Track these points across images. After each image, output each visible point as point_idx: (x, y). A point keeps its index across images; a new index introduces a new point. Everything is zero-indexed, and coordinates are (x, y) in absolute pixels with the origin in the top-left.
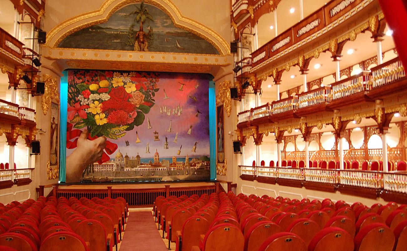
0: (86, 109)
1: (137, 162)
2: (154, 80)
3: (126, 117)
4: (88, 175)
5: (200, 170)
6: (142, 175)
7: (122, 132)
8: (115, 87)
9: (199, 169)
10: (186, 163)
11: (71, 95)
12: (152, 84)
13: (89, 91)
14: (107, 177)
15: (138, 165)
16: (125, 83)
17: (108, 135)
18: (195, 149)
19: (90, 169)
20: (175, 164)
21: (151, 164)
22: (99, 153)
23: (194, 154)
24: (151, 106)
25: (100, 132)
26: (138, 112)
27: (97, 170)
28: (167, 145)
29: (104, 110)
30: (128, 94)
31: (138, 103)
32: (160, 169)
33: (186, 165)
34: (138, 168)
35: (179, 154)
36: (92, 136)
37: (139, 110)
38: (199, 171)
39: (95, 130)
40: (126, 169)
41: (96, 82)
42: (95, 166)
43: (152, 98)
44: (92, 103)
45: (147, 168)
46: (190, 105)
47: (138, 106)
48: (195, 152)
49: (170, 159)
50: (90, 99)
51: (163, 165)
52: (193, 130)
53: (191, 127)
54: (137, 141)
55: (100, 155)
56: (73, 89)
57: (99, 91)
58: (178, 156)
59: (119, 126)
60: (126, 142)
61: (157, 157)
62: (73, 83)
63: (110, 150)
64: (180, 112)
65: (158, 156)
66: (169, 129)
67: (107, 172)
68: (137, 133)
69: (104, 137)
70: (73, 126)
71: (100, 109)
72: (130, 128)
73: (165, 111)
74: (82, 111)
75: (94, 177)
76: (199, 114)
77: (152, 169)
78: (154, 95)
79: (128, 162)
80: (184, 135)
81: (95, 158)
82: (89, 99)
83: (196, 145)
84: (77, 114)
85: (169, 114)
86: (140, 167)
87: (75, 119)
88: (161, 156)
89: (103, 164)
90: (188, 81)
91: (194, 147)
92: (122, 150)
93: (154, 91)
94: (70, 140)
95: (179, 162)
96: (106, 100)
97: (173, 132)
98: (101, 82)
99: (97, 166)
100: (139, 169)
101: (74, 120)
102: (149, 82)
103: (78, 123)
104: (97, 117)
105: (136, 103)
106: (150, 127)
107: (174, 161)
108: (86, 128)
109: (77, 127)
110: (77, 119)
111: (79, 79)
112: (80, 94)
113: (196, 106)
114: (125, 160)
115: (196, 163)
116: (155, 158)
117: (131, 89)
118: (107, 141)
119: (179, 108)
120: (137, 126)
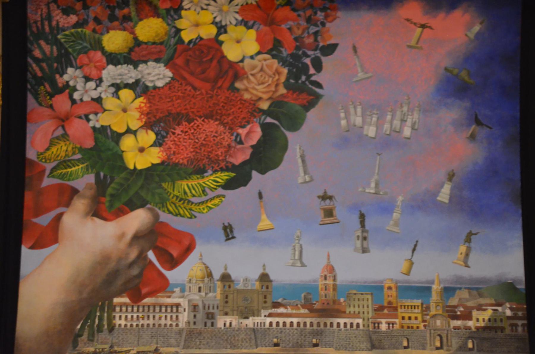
0: (91, 117)
1: (261, 298)
2: (320, 15)
3: (225, 143)
4: (91, 339)
5: (485, 335)
6: (277, 345)
7: (211, 194)
8: (186, 40)
9: (484, 328)
10: (433, 306)
11: (41, 69)
12: (313, 29)
13: (99, 54)
14: (156, 350)
15: (264, 308)
16: (222, 29)
17: (163, 203)
18: (467, 255)
19: (101, 319)
20: (393, 308)
21: (308, 305)
22: (131, 265)
23: (465, 273)
24: (309, 106)
25: (137, 193)
26: (265, 127)
27: (123, 322)
28: (365, 238)
29: (153, 119)
30: (232, 65)
31: (265, 96)
32: (338, 324)
33: (433, 312)
35: (408, 274)
36: (111, 206)
37: (269, 120)
38: (484, 339)
39: (121, 185)
40: (221, 321)
41: (126, 23)
42: (118, 309)
43: (313, 78)
44: (110, 96)
45: (295, 320)
46: (449, 101)
47: (265, 106)
48: (467, 266)
49: (376, 289)
50: (105, 84)
51: (352, 309)
53: (451, 177)
55: (135, 271)
56: (47, 48)
57: (131, 56)
58: (406, 277)
59: (201, 172)
60: (225, 228)
62: (47, 28)
63: (171, 255)
64: (409, 122)
65: (334, 280)
66: (373, 185)
67: (158, 332)
68: (260, 196)
69: (150, 209)
70: (48, 172)
71: (137, 115)
72: (239, 179)
73: (359, 121)
74: (77, 120)
75: (111, 347)
76: (482, 132)
77: (312, 324)
78: (318, 66)
79: (230, 297)
80: (424, 204)
81: (119, 282)
82: (100, 81)
83: (468, 240)
84: (60, 132)
85: (371, 131)
86: (270, 315)
87: (54, 149)
89: (147, 301)
90: (442, 15)
91: (463, 249)
92: (211, 256)
93: (318, 53)
94: (35, 220)
95: (408, 302)
96: (160, 84)
97: (386, 194)
98: (141, 23)
99: (124, 309)
100: (268, 320)
101: (49, 153)
102: (303, 23)
103: (65, 163)
104: (128, 143)
105: (260, 95)
106: (307, 178)
107: (390, 296)
108: (91, 178)
109: (62, 177)
110: (61, 150)
111: (67, 12)
112: (72, 66)
113: (467, 104)
114: (219, 291)
115: (473, 308)
116: (321, 283)
117: (242, 46)
118: (162, 222)
119: (405, 109)
120: (263, 171)
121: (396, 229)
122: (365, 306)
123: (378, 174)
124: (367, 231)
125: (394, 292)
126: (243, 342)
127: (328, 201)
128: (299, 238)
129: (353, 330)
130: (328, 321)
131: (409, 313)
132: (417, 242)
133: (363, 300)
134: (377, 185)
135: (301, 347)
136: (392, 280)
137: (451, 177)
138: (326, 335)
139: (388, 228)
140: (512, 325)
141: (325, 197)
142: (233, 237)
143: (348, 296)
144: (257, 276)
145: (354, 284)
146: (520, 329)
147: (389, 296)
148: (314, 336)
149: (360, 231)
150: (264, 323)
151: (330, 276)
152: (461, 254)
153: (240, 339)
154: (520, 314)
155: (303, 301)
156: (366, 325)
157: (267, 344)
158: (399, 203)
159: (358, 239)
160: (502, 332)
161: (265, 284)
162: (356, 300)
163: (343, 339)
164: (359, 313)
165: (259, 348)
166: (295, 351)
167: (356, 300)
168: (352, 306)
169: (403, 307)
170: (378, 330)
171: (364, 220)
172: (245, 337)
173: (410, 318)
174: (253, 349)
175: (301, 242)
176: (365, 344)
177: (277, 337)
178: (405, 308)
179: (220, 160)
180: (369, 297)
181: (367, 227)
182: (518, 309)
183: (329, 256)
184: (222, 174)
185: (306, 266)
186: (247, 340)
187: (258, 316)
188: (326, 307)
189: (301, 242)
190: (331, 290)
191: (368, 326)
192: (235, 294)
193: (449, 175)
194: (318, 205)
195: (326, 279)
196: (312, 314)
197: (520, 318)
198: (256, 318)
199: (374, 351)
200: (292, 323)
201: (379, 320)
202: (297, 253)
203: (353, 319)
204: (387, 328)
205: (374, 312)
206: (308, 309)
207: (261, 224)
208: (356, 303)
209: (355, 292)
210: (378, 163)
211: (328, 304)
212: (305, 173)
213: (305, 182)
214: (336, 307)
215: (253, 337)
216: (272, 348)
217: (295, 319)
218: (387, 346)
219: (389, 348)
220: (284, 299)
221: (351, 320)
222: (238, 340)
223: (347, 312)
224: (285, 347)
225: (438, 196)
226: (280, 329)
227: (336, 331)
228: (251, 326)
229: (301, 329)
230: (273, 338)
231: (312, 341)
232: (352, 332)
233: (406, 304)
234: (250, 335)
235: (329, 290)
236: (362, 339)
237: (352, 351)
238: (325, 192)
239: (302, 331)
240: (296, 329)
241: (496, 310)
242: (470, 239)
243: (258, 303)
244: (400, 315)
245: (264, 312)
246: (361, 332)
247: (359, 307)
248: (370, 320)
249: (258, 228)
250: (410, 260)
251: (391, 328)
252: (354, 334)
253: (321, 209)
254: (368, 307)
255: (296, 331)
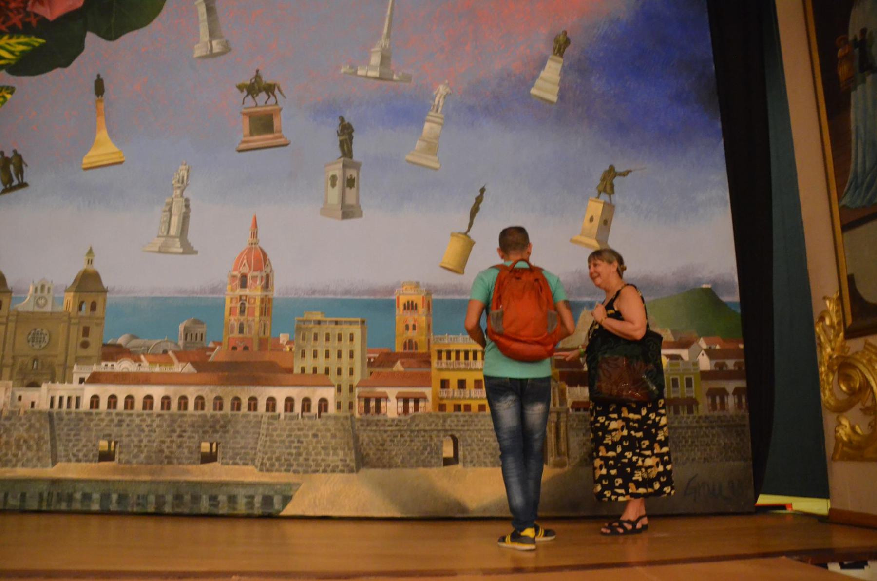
6: (106, 456)
15: (78, 360)
18: (606, 223)
32: (271, 403)
34: (77, 390)
35: (459, 269)
45: (158, 392)
49: (376, 308)
51: (309, 363)
52: (578, 71)
53: (561, 46)
54: (93, 156)
58: (454, 279)
61: (254, 292)
65: (267, 286)
66: (375, 60)
68: (99, 88)
77: (200, 402)
80: (501, 102)
83: (608, 184)
86: (95, 379)
88: (291, 278)
91: (596, 208)
97: (407, 78)
100: (90, 391)
106: (217, 47)
116: (230, 295)
120: (111, 34)
121: (431, 161)
122: (345, 355)
123: (389, 35)
124: (357, 166)
125: (421, 317)
126: (19, 447)
127: (263, 96)
128: (183, 184)
129: (310, 418)
130: (245, 394)
131: (459, 370)
132: (483, 190)
133: (340, 339)
134: (385, 60)
135: (170, 463)
136: (417, 285)
137: (561, 46)
138: (237, 432)
139: (409, 157)
140: (712, 393)
141: (254, 88)
142: (23, 185)
143: (299, 329)
144: (69, 277)
145: (317, 296)
146: (731, 401)
147: (407, 328)
148: (205, 432)
149: (341, 165)
150: (78, 399)
151: (254, 278)
152: (591, 220)
153: (12, 440)
154: (731, 364)
155: (181, 343)
156: (345, 406)
157: (81, 455)
158: (439, 100)
159: (333, 185)
160: (690, 411)
161: (89, 299)
162: (322, 339)
163: (283, 442)
164: (327, 371)
165: (59, 464)
166: (152, 473)
167: (322, 339)
168: (309, 354)
169: (444, 355)
170: (376, 417)
171: (351, 138)
172: (25, 435)
173: (462, 384)
174: (44, 466)
175: (186, 194)
176: (341, 453)
177: (107, 436)
178: (449, 357)
179: (11, 10)
180: (357, 331)
181: (356, 157)
182: (724, 354)
183: (255, 225)
184: (13, 41)
185: (196, 252)
186: (32, 442)
187: (63, 381)
188: (240, 356)
189: (186, 195)
190: (257, 313)
191: (351, 406)
192: (11, 325)
193: (556, 40)
194: (238, 105)
195: (243, 285)
196: (205, 376)
197: (730, 376)
198: (58, 385)
199: (365, 472)
200: (149, 399)
201: (380, 390)
202: (175, 220)
203: (311, 389)
204: (401, 410)
205: (367, 370)
206: (192, 363)
207: (89, 154)
208: (321, 346)
209: (319, 317)
210: (389, 12)
211: (246, 348)
212: (212, 35)
213: (212, 55)
214: (268, 357)
215: (47, 437)
216: (93, 464)
217: (159, 388)
218: (399, 460)
219: (404, 464)
220: (134, 337)
221: (306, 392)
222: (7, 443)
223: (297, 370)
224: (128, 462)
225: (532, 86)
226: (118, 414)
227: (265, 419)
228: (45, 406)
229: (171, 415)
230: (98, 438)
231: (199, 447)
232: (306, 421)
233: (453, 347)
234: (38, 431)
235: (253, 315)
236: (333, 441)
237: (306, 472)
238: (258, 76)
239: (173, 419)
240: (159, 415)
241: (678, 357)
242: (612, 186)
243: (67, 349)
244: (436, 377)
245: (80, 371)
246: (331, 423)
247: (327, 355)
248: (357, 391)
249: (85, 161)
250: (466, 234)
251: (411, 410)
252: (311, 427)
253: (245, 114)
254: (352, 356)
255: (158, 421)
